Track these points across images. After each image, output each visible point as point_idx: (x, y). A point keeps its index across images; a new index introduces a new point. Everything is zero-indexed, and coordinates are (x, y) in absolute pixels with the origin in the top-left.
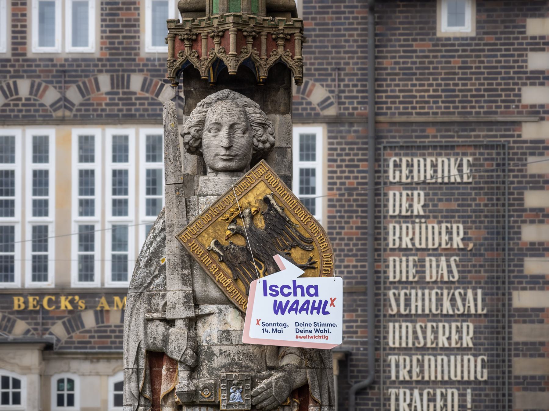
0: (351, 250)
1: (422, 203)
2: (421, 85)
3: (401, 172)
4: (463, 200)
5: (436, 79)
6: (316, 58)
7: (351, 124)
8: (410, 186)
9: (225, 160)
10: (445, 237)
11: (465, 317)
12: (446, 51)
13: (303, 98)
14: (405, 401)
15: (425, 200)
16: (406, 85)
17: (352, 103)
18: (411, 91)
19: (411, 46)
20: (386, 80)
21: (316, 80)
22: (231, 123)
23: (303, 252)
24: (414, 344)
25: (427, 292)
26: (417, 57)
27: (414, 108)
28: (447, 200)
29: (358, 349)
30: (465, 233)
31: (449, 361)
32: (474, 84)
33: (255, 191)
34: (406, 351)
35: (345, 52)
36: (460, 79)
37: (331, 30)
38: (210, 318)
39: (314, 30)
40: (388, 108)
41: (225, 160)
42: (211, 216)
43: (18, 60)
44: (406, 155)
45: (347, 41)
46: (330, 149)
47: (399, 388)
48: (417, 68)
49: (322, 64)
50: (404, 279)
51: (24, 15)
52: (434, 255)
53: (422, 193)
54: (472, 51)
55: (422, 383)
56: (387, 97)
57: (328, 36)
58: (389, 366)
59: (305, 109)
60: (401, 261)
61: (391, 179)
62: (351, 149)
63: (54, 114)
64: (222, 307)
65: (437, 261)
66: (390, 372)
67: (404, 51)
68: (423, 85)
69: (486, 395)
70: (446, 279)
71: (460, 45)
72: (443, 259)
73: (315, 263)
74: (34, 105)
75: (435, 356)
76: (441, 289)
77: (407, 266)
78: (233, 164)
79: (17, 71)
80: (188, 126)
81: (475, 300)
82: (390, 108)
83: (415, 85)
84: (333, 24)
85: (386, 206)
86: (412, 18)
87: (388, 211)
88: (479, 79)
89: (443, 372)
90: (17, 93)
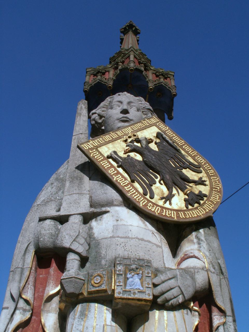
22: (129, 101)
23: (194, 173)
38: (105, 216)
42: (112, 137)
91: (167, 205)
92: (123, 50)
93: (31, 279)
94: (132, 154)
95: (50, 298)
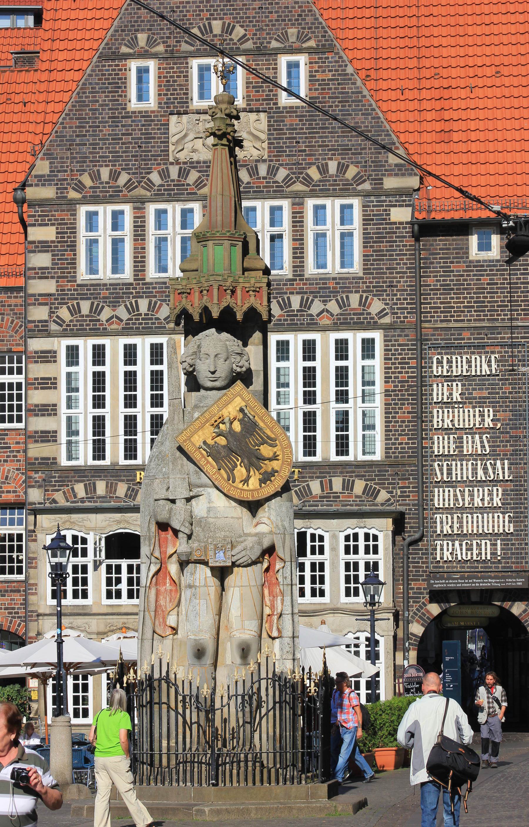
0: (404, 430)
1: (460, 392)
2: (457, 298)
3: (442, 367)
4: (492, 389)
5: (470, 293)
6: (373, 278)
7: (403, 330)
8: (449, 379)
10: (478, 419)
11: (495, 482)
12: (477, 271)
13: (364, 310)
14: (448, 550)
15: (462, 389)
16: (447, 298)
17: (404, 313)
18: (450, 303)
19: (450, 267)
20: (430, 294)
21: (375, 295)
24: (454, 505)
25: (464, 463)
26: (454, 276)
27: (453, 316)
28: (479, 389)
29: (410, 510)
30: (494, 415)
31: (483, 518)
32: (500, 297)
33: (233, 403)
34: (449, 510)
35: (397, 273)
36: (488, 293)
37: (386, 255)
39: (372, 256)
40: (431, 317)
43: (139, 284)
44: (446, 354)
45: (397, 264)
46: (385, 350)
47: (443, 540)
48: (454, 285)
49: (379, 282)
50: (446, 453)
51: (144, 248)
52: (470, 434)
53: (459, 384)
54: (497, 270)
55: (462, 536)
56: (430, 308)
57: (383, 260)
58: (436, 522)
59: (366, 318)
60: (444, 439)
61: (435, 373)
62: (402, 350)
63: (167, 326)
65: (472, 438)
66: (436, 527)
67: (444, 271)
68: (460, 298)
69: (513, 544)
70: (480, 452)
71: (488, 266)
72: (477, 436)
74: (152, 319)
75: (472, 514)
76: (476, 460)
77: (449, 443)
78: (218, 384)
79: (139, 292)
81: (503, 469)
82: (434, 317)
83: (453, 298)
84: (387, 251)
85: (431, 395)
86: (450, 245)
87: (432, 399)
88: (503, 293)
89: (478, 527)
90: (138, 310)
91: (245, 487)
92: (208, 235)
93: (157, 542)
94: (218, 439)
95: (171, 556)
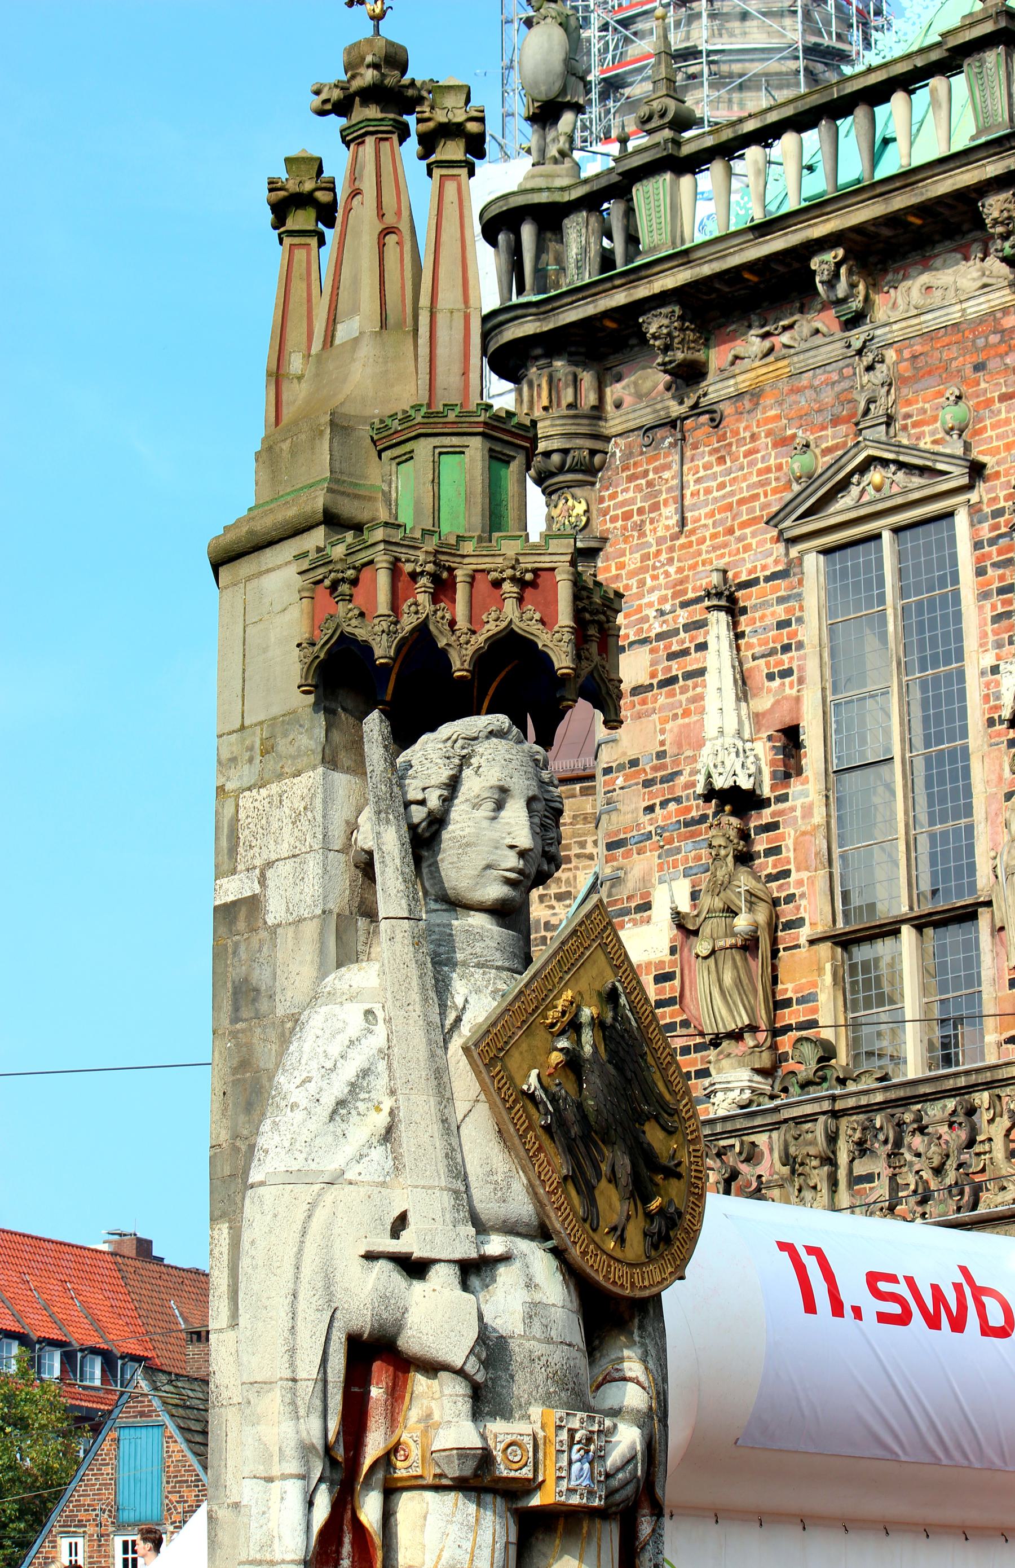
9: (508, 882)
22: (531, 794)
38: (502, 1270)
41: (508, 882)
64: (524, 1246)
73: (680, 1163)
80: (422, 785)
